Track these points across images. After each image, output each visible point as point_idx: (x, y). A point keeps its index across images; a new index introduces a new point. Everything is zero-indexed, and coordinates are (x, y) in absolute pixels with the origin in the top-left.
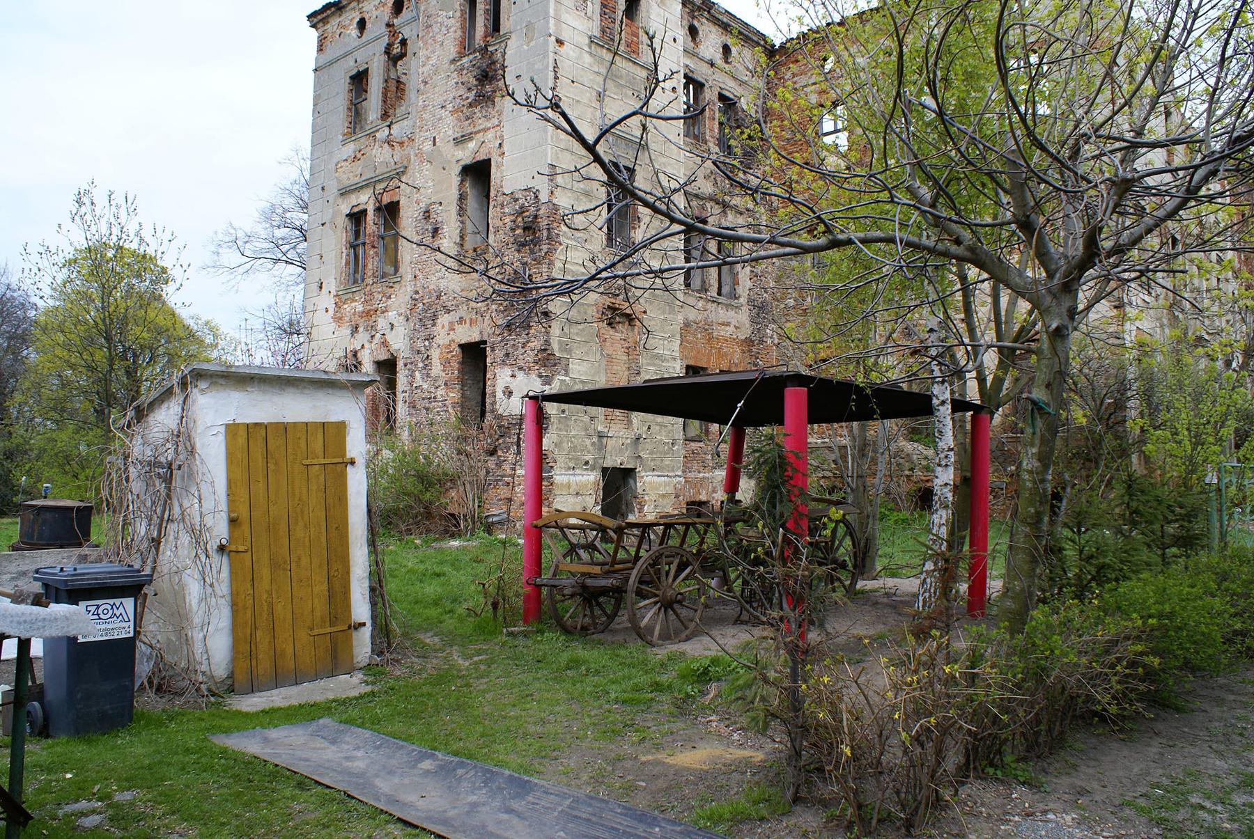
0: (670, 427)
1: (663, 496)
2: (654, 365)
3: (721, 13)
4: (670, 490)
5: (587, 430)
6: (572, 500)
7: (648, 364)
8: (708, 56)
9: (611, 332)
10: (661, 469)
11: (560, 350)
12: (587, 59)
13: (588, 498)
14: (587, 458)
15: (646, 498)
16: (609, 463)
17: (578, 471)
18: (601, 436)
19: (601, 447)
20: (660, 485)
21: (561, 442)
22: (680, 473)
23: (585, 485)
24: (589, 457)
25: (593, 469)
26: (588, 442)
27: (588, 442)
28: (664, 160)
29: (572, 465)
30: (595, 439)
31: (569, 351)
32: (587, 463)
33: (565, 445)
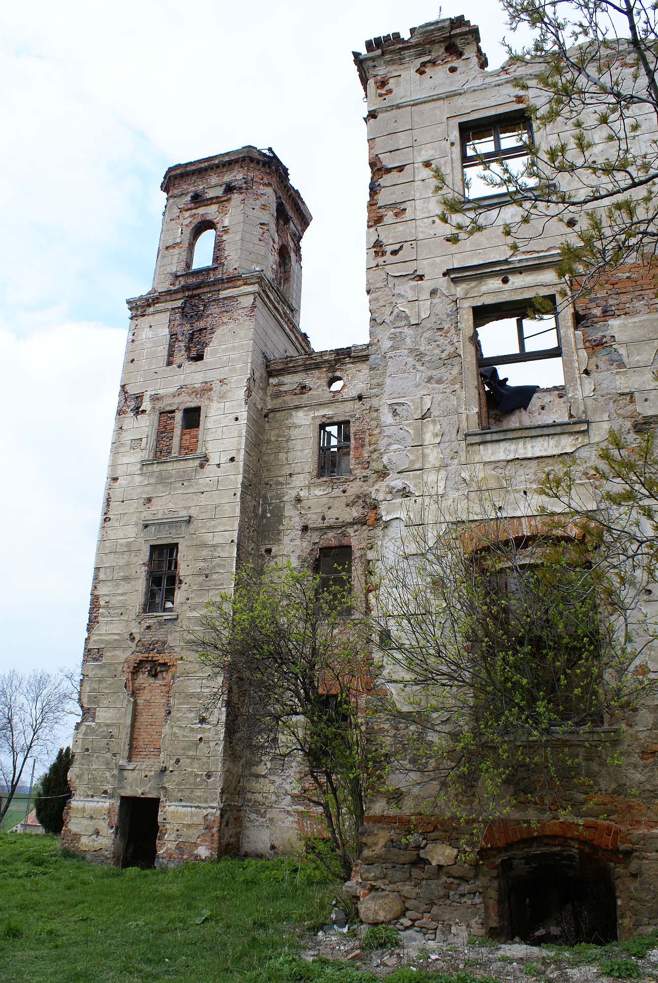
0: (205, 760)
1: (189, 826)
2: (189, 703)
3: (362, 350)
4: (199, 820)
5: (108, 764)
6: (85, 822)
7: (180, 704)
8: (355, 393)
9: (151, 680)
10: (190, 799)
11: (89, 702)
12: (138, 479)
13: (101, 822)
14: (105, 788)
15: (168, 826)
16: (128, 792)
17: (95, 799)
18: (122, 769)
19: (121, 778)
20: (185, 815)
21: (82, 775)
22: (215, 805)
23: (96, 810)
24: (109, 787)
25: (112, 797)
26: (108, 774)
27: (108, 774)
28: (213, 523)
29: (90, 793)
30: (116, 772)
31: (97, 703)
32: (105, 792)
33: (86, 777)
